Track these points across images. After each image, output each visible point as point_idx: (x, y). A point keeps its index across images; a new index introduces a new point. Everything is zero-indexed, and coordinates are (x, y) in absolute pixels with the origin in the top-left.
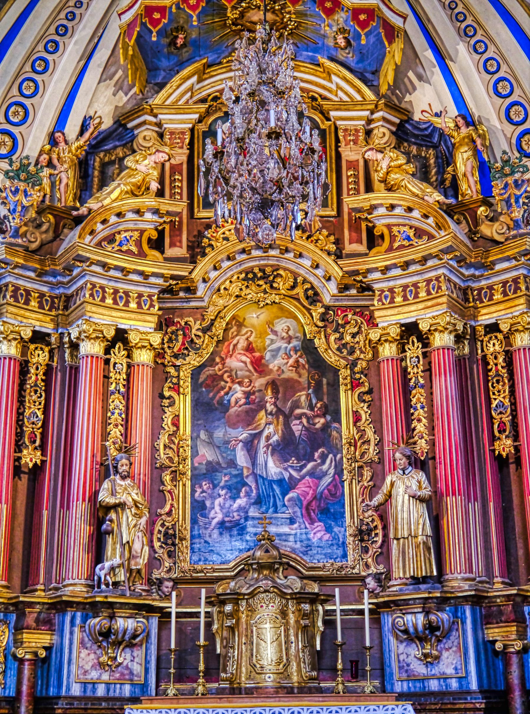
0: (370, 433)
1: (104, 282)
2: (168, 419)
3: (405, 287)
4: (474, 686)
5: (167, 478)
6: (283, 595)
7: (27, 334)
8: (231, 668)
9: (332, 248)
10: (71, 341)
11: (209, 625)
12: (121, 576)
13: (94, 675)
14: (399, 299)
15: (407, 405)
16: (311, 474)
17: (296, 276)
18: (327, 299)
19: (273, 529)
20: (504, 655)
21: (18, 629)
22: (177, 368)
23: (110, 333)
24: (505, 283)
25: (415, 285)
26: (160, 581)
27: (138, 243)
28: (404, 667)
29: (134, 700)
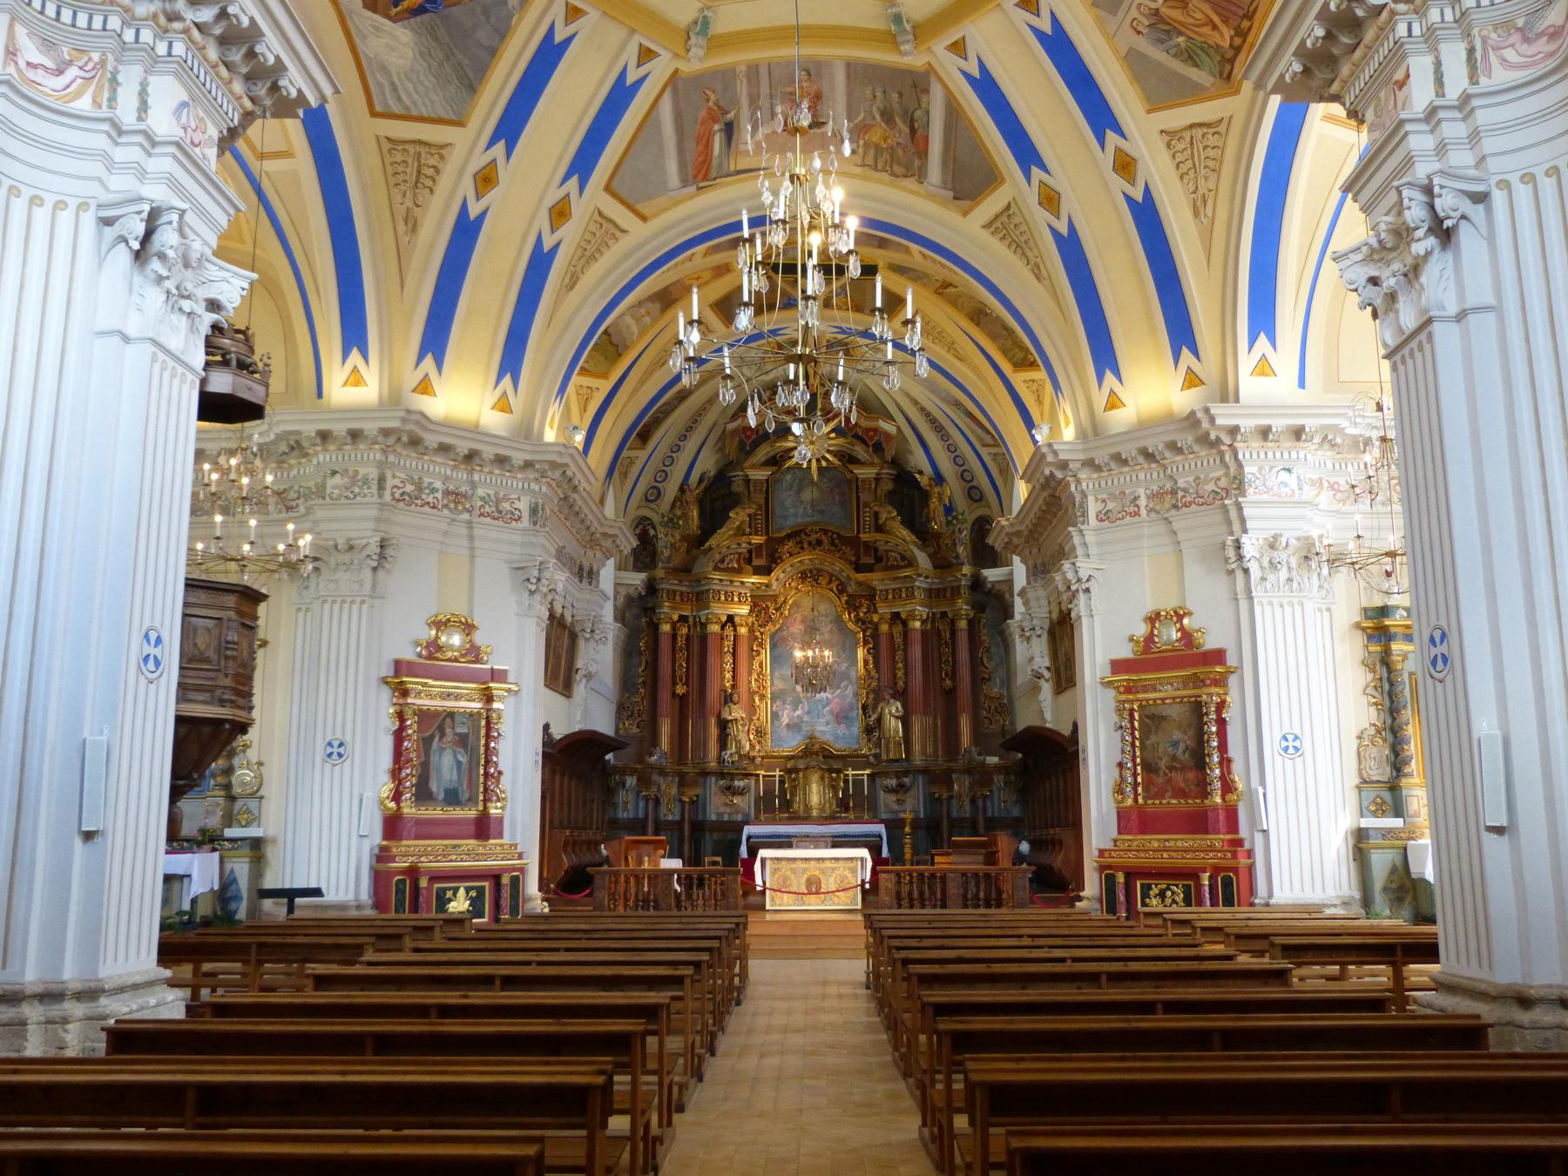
0: (873, 673)
1: (718, 588)
2: (756, 666)
3: (894, 590)
4: (922, 816)
5: (757, 699)
6: (821, 769)
7: (675, 617)
8: (796, 806)
9: (853, 559)
10: (701, 624)
11: (782, 782)
12: (736, 758)
13: (722, 809)
14: (890, 596)
15: (894, 662)
16: (838, 696)
17: (831, 575)
18: (850, 590)
19: (819, 728)
20: (939, 799)
21: (681, 785)
22: (762, 634)
23: (724, 619)
24: (952, 588)
25: (900, 589)
26: (754, 758)
27: (738, 562)
28: (886, 805)
29: (747, 823)
